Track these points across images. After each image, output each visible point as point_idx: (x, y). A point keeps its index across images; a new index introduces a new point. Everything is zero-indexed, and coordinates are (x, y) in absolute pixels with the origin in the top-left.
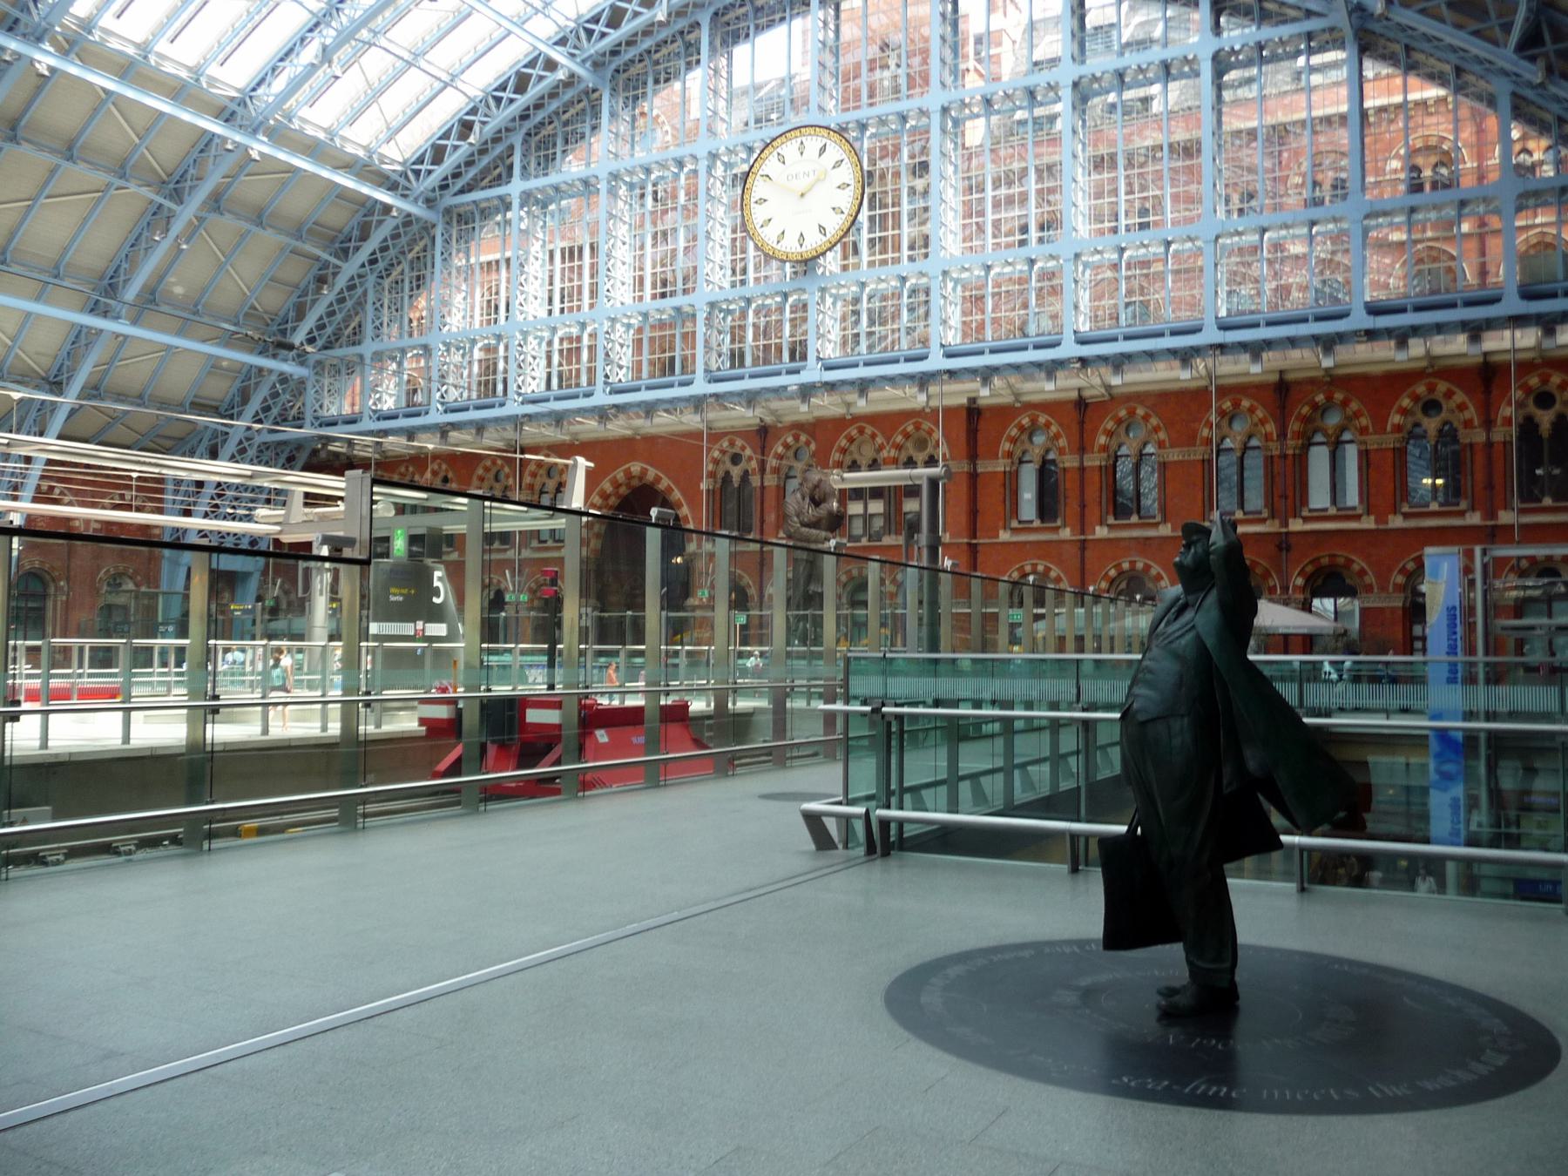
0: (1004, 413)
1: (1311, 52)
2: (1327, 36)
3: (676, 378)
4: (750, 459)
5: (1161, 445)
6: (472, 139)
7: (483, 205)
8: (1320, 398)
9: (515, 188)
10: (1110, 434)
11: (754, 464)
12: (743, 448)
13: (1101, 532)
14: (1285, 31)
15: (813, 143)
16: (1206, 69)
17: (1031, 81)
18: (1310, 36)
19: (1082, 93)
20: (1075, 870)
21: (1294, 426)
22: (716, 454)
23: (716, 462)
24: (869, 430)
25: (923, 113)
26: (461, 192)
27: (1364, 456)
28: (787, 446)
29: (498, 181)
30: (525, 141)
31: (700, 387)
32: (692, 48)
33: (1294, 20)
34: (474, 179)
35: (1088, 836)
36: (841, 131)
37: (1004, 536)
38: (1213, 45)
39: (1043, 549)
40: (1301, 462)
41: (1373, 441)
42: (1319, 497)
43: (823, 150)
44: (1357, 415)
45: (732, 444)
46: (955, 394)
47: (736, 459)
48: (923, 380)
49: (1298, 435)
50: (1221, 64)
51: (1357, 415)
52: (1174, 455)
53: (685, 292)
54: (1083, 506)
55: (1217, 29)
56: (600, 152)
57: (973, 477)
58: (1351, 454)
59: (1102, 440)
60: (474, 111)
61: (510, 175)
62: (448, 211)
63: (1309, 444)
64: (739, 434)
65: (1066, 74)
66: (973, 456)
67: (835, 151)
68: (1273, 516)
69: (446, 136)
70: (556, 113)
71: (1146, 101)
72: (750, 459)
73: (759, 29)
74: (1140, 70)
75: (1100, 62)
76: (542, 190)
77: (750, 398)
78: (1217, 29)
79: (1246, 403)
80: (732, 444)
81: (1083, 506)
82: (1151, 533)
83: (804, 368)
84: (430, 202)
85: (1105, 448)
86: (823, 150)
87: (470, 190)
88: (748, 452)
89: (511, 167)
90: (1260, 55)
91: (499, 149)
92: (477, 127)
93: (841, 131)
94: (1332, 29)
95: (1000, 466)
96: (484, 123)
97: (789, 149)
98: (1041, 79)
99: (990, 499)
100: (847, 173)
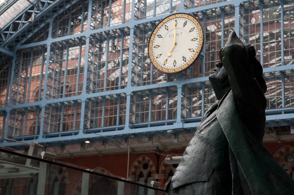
3: (117, 126)
4: (152, 166)
6: (30, 20)
7: (35, 49)
9: (49, 41)
11: (154, 169)
12: (149, 161)
15: (181, 21)
22: (136, 164)
23: (136, 167)
25: (232, 7)
26: (26, 43)
30: (54, 22)
31: (127, 130)
34: (31, 38)
36: (195, 15)
43: (185, 24)
45: (144, 159)
47: (146, 166)
53: (123, 87)
60: (32, 8)
61: (47, 36)
62: (19, 52)
67: (192, 24)
69: (19, 19)
70: (69, 9)
72: (152, 166)
76: (61, 43)
77: (150, 136)
80: (144, 159)
83: (175, 122)
84: (11, 48)
86: (185, 24)
87: (29, 43)
88: (151, 163)
89: (47, 33)
91: (43, 25)
92: (33, 16)
93: (195, 15)
96: (36, 13)
97: (171, 24)
100: (197, 34)
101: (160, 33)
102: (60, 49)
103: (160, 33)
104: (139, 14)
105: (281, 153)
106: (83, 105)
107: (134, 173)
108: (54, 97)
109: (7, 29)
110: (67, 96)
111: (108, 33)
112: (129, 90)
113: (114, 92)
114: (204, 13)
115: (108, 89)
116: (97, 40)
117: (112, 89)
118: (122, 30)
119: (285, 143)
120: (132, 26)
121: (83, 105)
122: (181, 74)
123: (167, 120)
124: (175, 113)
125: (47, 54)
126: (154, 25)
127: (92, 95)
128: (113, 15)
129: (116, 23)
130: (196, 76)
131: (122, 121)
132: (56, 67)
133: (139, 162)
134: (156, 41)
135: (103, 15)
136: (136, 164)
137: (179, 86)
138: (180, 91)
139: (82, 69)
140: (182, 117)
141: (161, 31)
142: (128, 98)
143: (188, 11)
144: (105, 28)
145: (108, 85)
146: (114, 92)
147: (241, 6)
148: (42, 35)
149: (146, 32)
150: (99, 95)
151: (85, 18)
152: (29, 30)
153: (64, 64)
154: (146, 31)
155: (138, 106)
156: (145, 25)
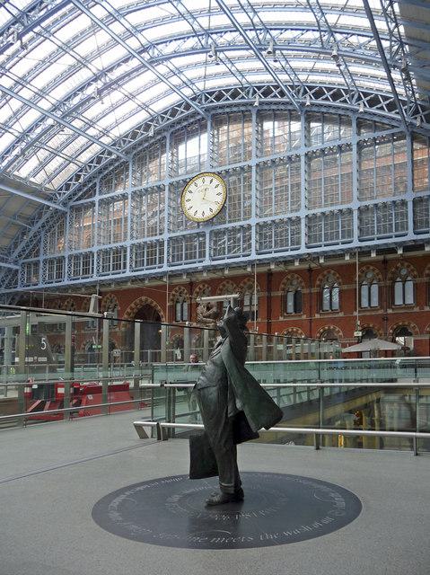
0: (281, 274)
1: (395, 140)
2: (400, 135)
5: (340, 284)
8: (399, 265)
9: (97, 198)
10: (321, 280)
13: (317, 316)
14: (384, 133)
15: (208, 179)
16: (355, 148)
17: (290, 154)
18: (393, 135)
19: (309, 157)
20: (318, 448)
21: (390, 275)
22: (174, 292)
23: (174, 295)
24: (231, 282)
25: (250, 167)
26: (77, 200)
27: (415, 286)
28: (200, 289)
29: (91, 196)
31: (166, 268)
32: (163, 146)
33: (388, 129)
34: (82, 195)
35: (323, 434)
36: (219, 173)
37: (281, 319)
38: (357, 139)
39: (295, 324)
40: (392, 289)
41: (418, 280)
42: (398, 301)
43: (211, 181)
44: (413, 271)
46: (264, 269)
48: (251, 263)
49: (391, 279)
50: (360, 146)
51: (413, 271)
52: (345, 287)
53: (161, 234)
54: (311, 307)
55: (359, 134)
56: (128, 186)
57: (269, 298)
58: (410, 285)
59: (318, 282)
60: (81, 171)
62: (71, 207)
63: (394, 282)
64: (183, 285)
65: (302, 151)
66: (269, 290)
67: (216, 182)
68: (381, 308)
69: (71, 180)
71: (336, 160)
73: (189, 138)
74: (330, 149)
75: (316, 145)
78: (359, 134)
79: (371, 268)
81: (311, 307)
82: (336, 316)
84: (65, 204)
85: (319, 286)
86: (211, 181)
90: (374, 141)
94: (401, 132)
95: (280, 293)
97: (199, 182)
98: (294, 153)
99: (276, 306)
100: (220, 189)
101: (190, 189)
102: (106, 203)
103: (190, 189)
104: (173, 174)
105: (288, 279)
106: (129, 250)
107: (172, 300)
108: (104, 244)
109: (61, 189)
110: (114, 242)
111: (146, 190)
112: (166, 236)
113: (154, 238)
114: (227, 172)
115: (148, 236)
116: (138, 195)
117: (152, 235)
118: (159, 187)
119: (290, 272)
120: (166, 184)
121: (129, 250)
122: (209, 222)
123: (198, 259)
124: (205, 253)
125: (97, 207)
126: (186, 183)
127: (135, 241)
128: (150, 174)
129: (152, 181)
130: (220, 224)
131: (161, 261)
132: (104, 219)
133: (176, 291)
134: (187, 196)
135: (142, 174)
136: (174, 292)
137: (208, 231)
138: (208, 236)
139: (126, 219)
140: (210, 256)
141: (192, 187)
142: (166, 243)
143: (213, 170)
144: (145, 185)
145: (148, 231)
146: (154, 238)
147: (257, 165)
148: (91, 192)
149: (178, 188)
150: (141, 241)
151: (127, 177)
152: (80, 190)
153: (111, 216)
154: (180, 188)
155: (174, 248)
156: (178, 183)
